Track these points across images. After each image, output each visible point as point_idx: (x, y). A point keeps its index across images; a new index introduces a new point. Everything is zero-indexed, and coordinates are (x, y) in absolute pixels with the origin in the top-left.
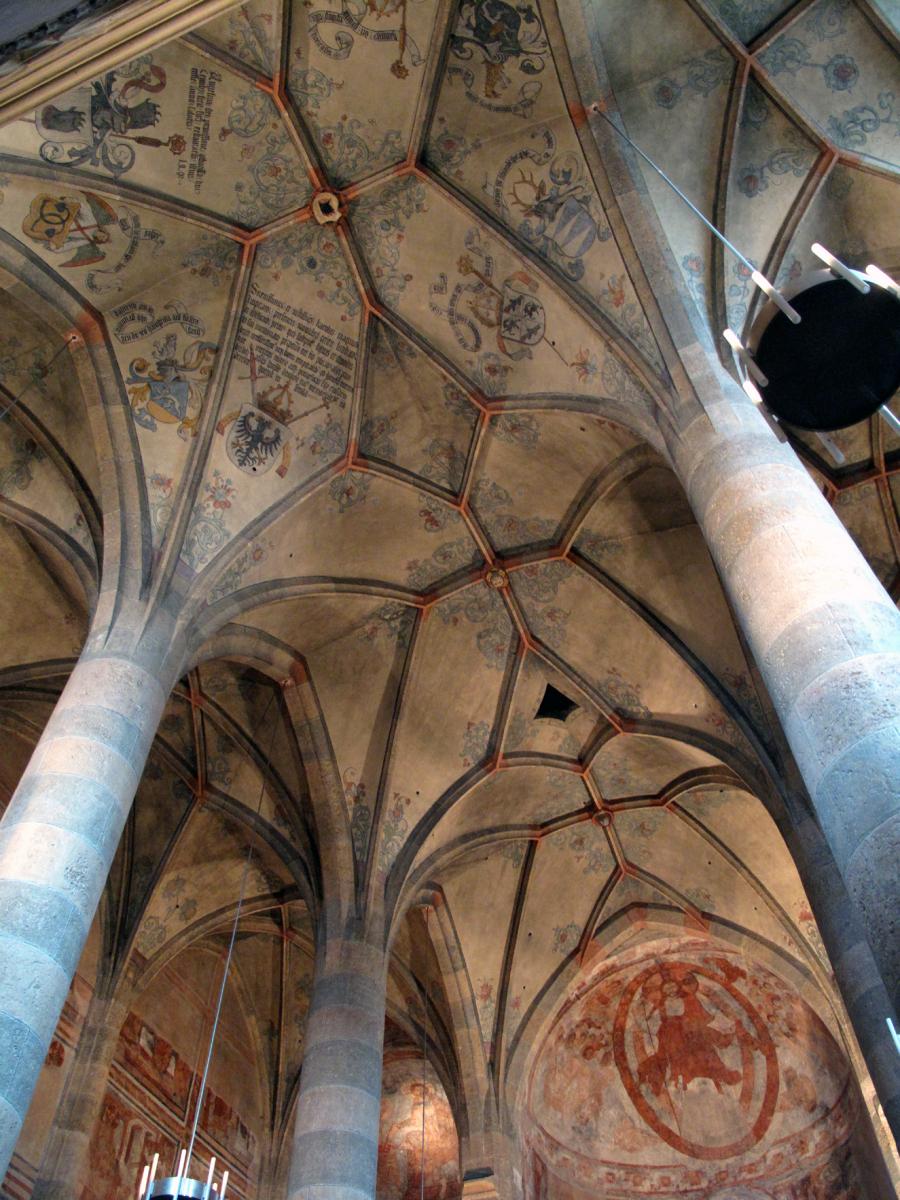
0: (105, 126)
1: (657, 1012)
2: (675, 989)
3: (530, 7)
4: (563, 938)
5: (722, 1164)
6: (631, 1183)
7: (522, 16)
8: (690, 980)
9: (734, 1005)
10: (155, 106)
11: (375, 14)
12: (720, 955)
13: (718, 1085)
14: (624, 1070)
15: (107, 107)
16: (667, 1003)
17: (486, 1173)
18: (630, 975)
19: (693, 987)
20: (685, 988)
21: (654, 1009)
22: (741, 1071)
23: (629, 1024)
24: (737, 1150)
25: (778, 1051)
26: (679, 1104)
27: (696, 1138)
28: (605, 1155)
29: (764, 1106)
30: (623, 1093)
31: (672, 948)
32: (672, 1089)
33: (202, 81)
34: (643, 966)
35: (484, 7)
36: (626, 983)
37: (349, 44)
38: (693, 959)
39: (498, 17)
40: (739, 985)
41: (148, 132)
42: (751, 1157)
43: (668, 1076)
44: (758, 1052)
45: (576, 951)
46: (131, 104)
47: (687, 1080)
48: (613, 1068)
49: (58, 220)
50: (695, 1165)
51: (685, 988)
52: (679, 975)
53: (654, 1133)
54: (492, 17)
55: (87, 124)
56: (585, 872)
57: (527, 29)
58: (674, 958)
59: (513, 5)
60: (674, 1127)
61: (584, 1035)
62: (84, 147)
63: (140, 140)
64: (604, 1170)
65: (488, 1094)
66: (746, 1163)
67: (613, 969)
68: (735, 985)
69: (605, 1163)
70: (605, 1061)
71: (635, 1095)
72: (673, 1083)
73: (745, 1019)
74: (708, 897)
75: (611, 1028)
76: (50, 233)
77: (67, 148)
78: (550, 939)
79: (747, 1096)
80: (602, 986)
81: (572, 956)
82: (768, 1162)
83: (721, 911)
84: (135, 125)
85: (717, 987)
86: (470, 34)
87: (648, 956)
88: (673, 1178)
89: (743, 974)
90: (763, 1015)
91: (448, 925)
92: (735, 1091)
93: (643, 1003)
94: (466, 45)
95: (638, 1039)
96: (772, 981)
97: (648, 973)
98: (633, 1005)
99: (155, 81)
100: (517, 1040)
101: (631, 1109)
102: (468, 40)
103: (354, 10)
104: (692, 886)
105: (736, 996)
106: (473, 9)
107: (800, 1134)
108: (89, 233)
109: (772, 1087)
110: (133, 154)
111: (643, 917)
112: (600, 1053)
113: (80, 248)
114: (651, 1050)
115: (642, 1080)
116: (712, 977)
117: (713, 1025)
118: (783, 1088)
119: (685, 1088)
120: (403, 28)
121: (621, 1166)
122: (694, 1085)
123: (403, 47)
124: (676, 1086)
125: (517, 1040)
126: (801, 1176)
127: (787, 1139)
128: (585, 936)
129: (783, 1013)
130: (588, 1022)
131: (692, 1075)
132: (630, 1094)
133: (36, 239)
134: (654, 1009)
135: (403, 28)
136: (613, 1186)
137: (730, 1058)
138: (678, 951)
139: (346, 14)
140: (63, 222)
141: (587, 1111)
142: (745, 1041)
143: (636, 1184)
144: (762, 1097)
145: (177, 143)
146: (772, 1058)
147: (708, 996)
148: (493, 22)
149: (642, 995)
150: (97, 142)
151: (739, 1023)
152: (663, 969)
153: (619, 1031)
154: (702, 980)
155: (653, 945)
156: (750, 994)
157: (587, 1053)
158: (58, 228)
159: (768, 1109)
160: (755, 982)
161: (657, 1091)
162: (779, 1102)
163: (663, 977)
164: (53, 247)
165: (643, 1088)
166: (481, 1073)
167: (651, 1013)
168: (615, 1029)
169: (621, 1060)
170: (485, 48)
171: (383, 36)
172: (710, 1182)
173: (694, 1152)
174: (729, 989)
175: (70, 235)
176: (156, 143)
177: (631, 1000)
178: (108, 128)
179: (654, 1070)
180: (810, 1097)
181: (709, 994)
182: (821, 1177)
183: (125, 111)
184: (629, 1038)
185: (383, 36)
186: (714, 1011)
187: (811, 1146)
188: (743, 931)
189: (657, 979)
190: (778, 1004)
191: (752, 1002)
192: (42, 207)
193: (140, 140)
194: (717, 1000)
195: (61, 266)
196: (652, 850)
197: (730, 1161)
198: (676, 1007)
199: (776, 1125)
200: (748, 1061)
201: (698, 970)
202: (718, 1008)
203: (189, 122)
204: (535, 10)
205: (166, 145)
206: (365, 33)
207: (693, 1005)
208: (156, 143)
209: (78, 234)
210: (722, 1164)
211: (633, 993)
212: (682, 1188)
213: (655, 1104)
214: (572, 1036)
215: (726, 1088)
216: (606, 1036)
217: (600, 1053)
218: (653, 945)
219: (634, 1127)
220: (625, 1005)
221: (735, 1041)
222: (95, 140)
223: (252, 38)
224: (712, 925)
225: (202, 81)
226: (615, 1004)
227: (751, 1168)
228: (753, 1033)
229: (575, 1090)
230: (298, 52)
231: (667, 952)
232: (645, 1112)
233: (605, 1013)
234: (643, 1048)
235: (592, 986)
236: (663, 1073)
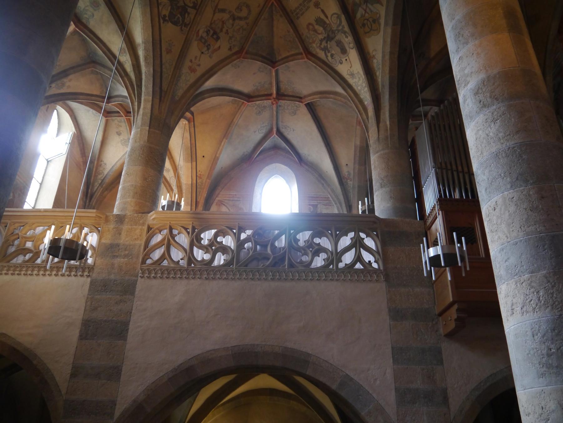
0: (333, 32)
3: (163, 23)
7: (167, 18)
10: (316, 21)
11: (223, 19)
15: (328, 35)
33: (297, 14)
35: (181, 22)
37: (238, 8)
39: (177, 17)
41: (322, 17)
46: (321, 29)
49: (369, 23)
54: (179, 18)
55: (337, 38)
57: (165, 12)
59: (170, 24)
62: (343, 34)
63: (327, 17)
76: (374, 21)
77: (347, 40)
84: (325, 23)
86: (189, 10)
94: (191, 5)
99: (311, 27)
102: (189, 7)
103: (231, 21)
106: (186, 21)
108: (364, 7)
110: (332, 15)
113: (372, 5)
120: (214, 14)
123: (217, 5)
133: (379, 24)
135: (214, 14)
139: (234, 20)
140: (368, 20)
145: (317, 5)
148: (179, 15)
150: (339, 31)
158: (371, 20)
164: (378, 15)
170: (184, 3)
171: (223, 11)
175: (370, 13)
176: (323, 11)
178: (332, 30)
183: (325, 29)
185: (223, 11)
192: (368, 32)
193: (327, 17)
195: (382, 5)
203: (308, 7)
204: (162, 21)
205: (320, 8)
206: (230, 12)
208: (323, 11)
209: (368, 10)
222: (338, 32)
223: (274, 12)
225: (297, 14)
230: (259, 6)
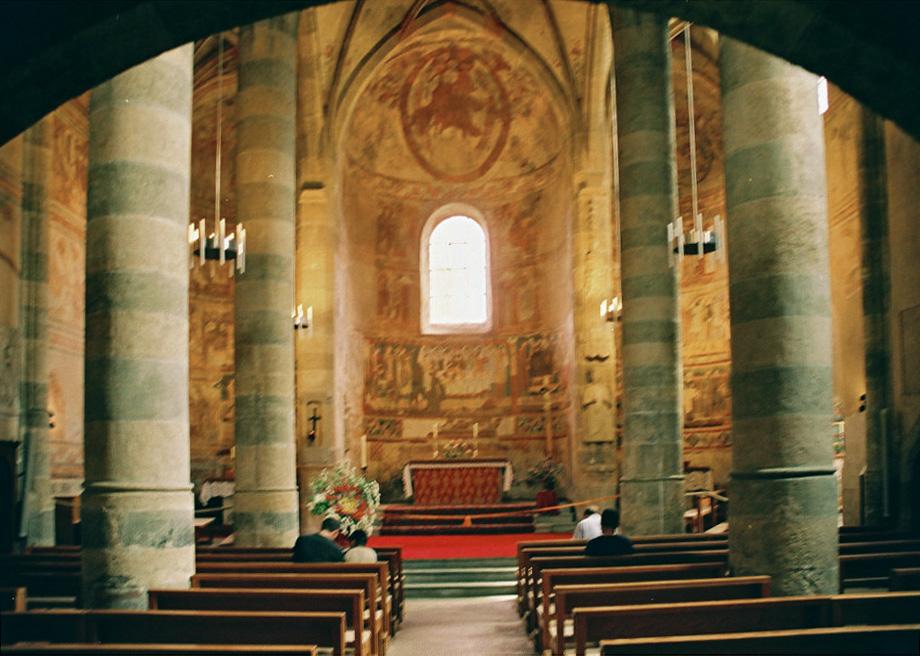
4: (390, 16)
5: (455, 186)
9: (492, 85)
12: (497, 51)
13: (464, 135)
16: (447, 73)
17: (318, 186)
18: (429, 50)
19: (469, 66)
23: (417, 82)
26: (434, 142)
27: (441, 167)
30: (400, 134)
32: (432, 131)
34: (439, 46)
36: (424, 54)
38: (478, 49)
40: (504, 76)
42: (474, 185)
43: (433, 121)
47: (445, 127)
48: (396, 112)
51: (464, 66)
52: (463, 57)
58: (464, 45)
60: (427, 156)
61: (384, 86)
65: (323, 129)
66: (471, 188)
67: (418, 44)
69: (381, 175)
70: (392, 105)
71: (407, 131)
73: (497, 95)
78: (382, 16)
79: (481, 146)
81: (395, 31)
85: (486, 70)
87: (445, 40)
89: (509, 68)
92: (475, 141)
93: (429, 70)
97: (442, 51)
100: (345, 90)
105: (497, 80)
109: (500, 144)
111: (455, 12)
112: (391, 100)
114: (425, 103)
115: (413, 123)
116: (486, 63)
118: (507, 147)
121: (389, 178)
122: (448, 132)
125: (345, 90)
126: (504, 203)
128: (407, 16)
129: (526, 101)
130: (389, 78)
137: (477, 119)
142: (492, 111)
146: (506, 126)
151: (491, 98)
152: (453, 50)
153: (407, 87)
154: (477, 64)
157: (382, 99)
159: (493, 158)
160: (515, 75)
161: (423, 131)
165: (413, 128)
166: (319, 114)
169: (403, 107)
173: (437, 175)
179: (424, 115)
180: (525, 157)
181: (479, 73)
184: (412, 93)
187: (515, 189)
188: (525, 45)
189: (446, 56)
198: (452, 77)
199: (496, 167)
200: (489, 124)
201: (475, 57)
207: (464, 78)
211: (426, 62)
212: (425, 197)
213: (419, 140)
214: (375, 86)
217: (391, 100)
218: (454, 33)
224: (505, 33)
226: (410, 69)
227: (472, 192)
228: (499, 106)
229: (371, 124)
231: (462, 40)
236: (429, 120)
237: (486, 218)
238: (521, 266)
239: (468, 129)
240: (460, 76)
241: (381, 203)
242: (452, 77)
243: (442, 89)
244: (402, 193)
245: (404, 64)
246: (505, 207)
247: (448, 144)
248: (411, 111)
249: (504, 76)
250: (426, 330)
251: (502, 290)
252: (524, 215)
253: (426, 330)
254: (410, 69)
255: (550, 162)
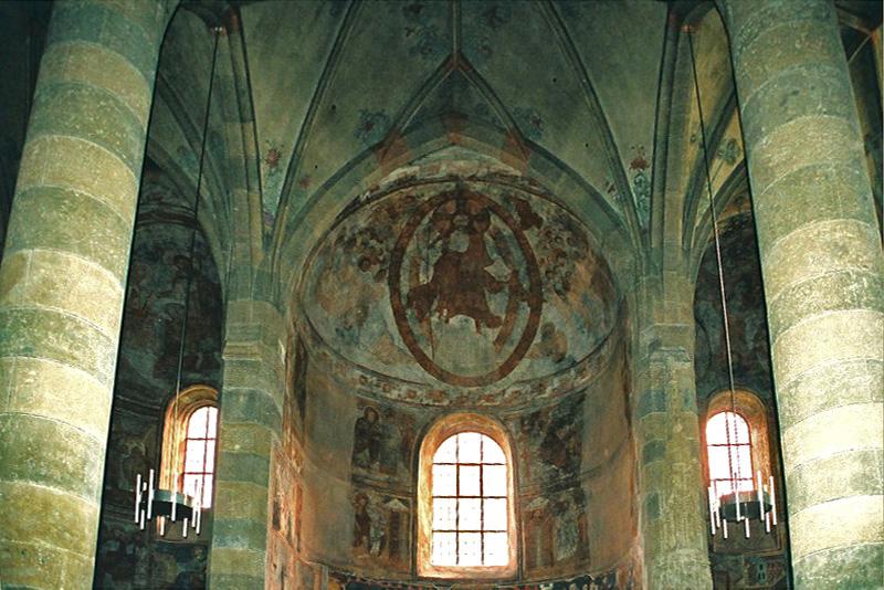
1: (440, 242)
2: (466, 224)
5: (465, 391)
6: (381, 389)
8: (484, 218)
9: (517, 254)
13: (477, 325)
14: (395, 291)
18: (428, 193)
20: (476, 224)
21: (439, 239)
22: (503, 317)
23: (410, 248)
24: (481, 382)
25: (544, 305)
26: (438, 334)
27: (448, 366)
28: (362, 361)
29: (515, 351)
31: (479, 175)
32: (434, 319)
34: (442, 187)
38: (495, 194)
40: (531, 236)
42: (492, 389)
43: (434, 307)
44: (525, 304)
45: (380, 145)
48: (385, 286)
50: (439, 386)
51: (476, 224)
53: (410, 353)
56: (412, 51)
60: (428, 352)
61: (365, 244)
64: (358, 373)
66: (487, 393)
68: (525, 233)
69: (360, 367)
70: (379, 277)
71: (399, 315)
72: (438, 314)
73: (522, 270)
74: (538, 122)
75: (392, 246)
80: (395, 196)
81: (373, 149)
82: (506, 396)
83: (546, 142)
85: (507, 232)
87: (452, 178)
88: (419, 393)
89: (538, 222)
90: (543, 270)
91: (240, 60)
92: (492, 334)
93: (429, 230)
95: (415, 265)
96: (566, 235)
97: (445, 197)
98: (420, 228)
101: (393, 328)
104: (525, 105)
107: (541, 379)
109: (528, 336)
112: (376, 268)
114: (423, 280)
115: (409, 304)
116: (505, 221)
117: (490, 269)
118: (537, 339)
119: (447, 321)
121: (374, 373)
124: (439, 317)
126: (533, 410)
127: (529, 381)
130: (371, 232)
131: (458, 311)
132: (395, 314)
134: (439, 239)
136: (364, 388)
137: (496, 304)
138: (483, 180)
141: (352, 320)
142: (516, 291)
143: (384, 391)
144: (516, 344)
146: (536, 311)
147: (494, 239)
149: (431, 221)
151: (516, 273)
153: (400, 251)
154: (495, 221)
155: (461, 166)
156: (537, 246)
157: (363, 264)
160: (548, 234)
161: (422, 317)
162: (530, 350)
163: (458, 206)
165: (409, 312)
167: (435, 242)
168: (395, 249)
172: (451, 402)
173: (442, 376)
174: (518, 236)
177: (419, 223)
179: (423, 298)
180: (561, 351)
181: (497, 236)
182: (550, 414)
184: (406, 262)
186: (495, 255)
187: (549, 389)
188: (563, 167)
189: (451, 206)
190: (561, 260)
191: (535, 253)
194: (502, 246)
196: (495, 48)
197: (473, 389)
198: (461, 242)
200: (512, 310)
201: (495, 209)
202: (500, 254)
210: (465, 391)
211: (423, 215)
212: (425, 402)
213: (417, 330)
214: (353, 241)
215: (485, 329)
216: (385, 253)
217: (376, 268)
219: (392, 344)
220: (412, 225)
221: (507, 290)
226: (402, 224)
227: (489, 398)
231: (473, 178)
232: (406, 333)
233: (390, 228)
234: (417, 275)
235: (385, 194)
236: (431, 303)
237: (508, 431)
238: (559, 488)
239: (483, 317)
240: (471, 241)
241: (362, 403)
242: (461, 242)
243: (448, 260)
244: (394, 394)
245: (394, 216)
246: (536, 415)
247: (462, 340)
248: (405, 290)
249: (531, 236)
250: (426, 570)
251: (531, 525)
252: (560, 423)
253: (426, 570)
254: (402, 224)
255: (598, 349)
